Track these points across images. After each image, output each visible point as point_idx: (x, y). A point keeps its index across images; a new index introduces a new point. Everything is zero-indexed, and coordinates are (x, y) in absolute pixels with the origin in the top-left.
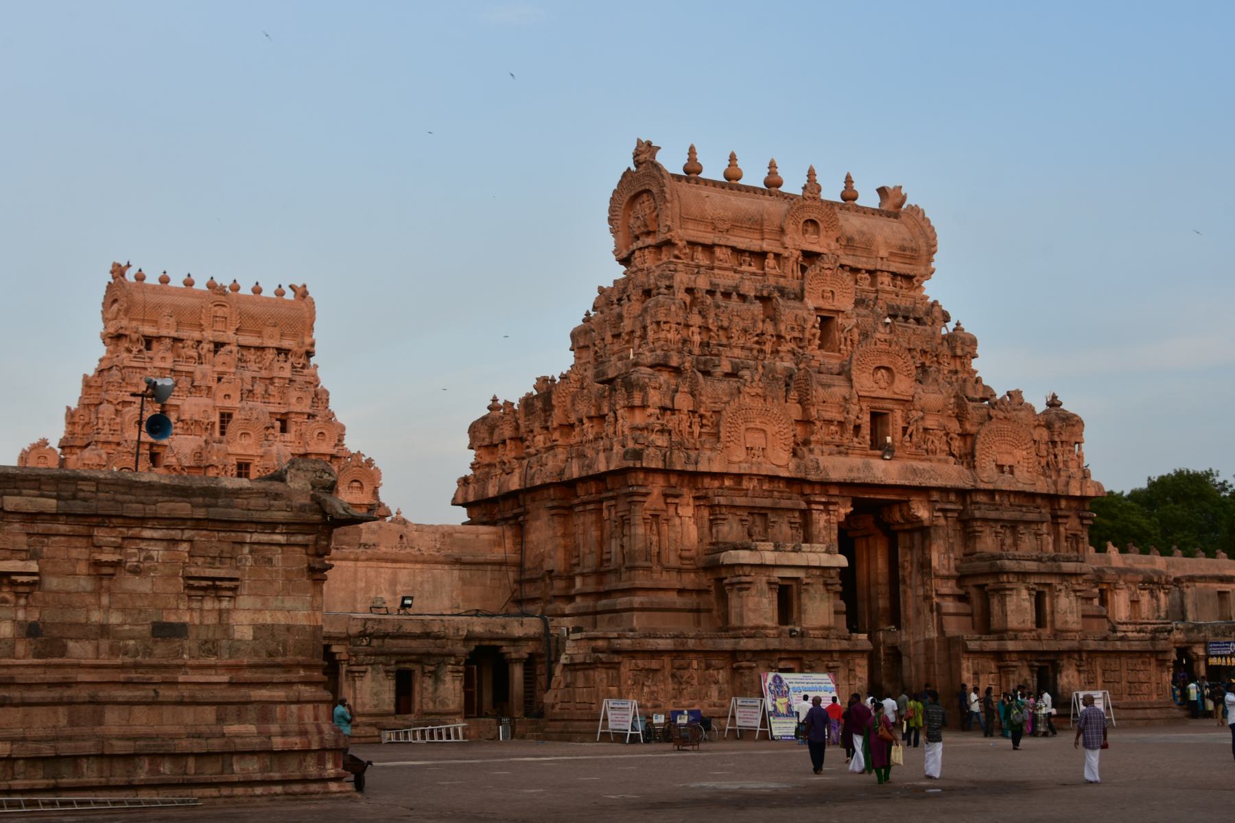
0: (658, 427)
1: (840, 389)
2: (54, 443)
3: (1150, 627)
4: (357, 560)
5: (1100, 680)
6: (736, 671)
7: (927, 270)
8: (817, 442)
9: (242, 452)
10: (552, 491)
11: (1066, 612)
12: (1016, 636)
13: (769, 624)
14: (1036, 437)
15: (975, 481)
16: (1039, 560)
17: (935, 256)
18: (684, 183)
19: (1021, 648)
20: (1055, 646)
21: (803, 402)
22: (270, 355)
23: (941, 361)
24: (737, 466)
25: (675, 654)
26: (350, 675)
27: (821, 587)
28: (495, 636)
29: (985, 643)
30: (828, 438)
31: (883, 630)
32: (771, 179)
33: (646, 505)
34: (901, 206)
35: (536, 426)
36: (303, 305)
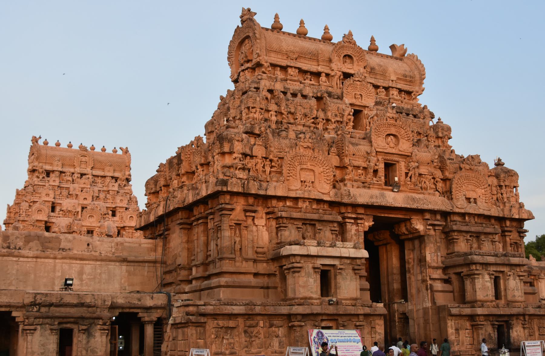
0: (240, 166)
1: (364, 147)
4: (55, 258)
5: (537, 334)
6: (291, 328)
7: (420, 89)
8: (350, 180)
9: (89, 225)
11: (514, 289)
12: (482, 305)
13: (314, 296)
14: (490, 183)
15: (453, 207)
16: (496, 255)
17: (424, 81)
18: (270, 32)
19: (486, 313)
20: (508, 311)
21: (340, 155)
23: (429, 140)
24: (294, 192)
25: (247, 317)
26: (25, 332)
27: (351, 271)
28: (133, 306)
29: (462, 310)
30: (357, 178)
31: (397, 303)
32: (325, 36)
33: (231, 216)
34: (404, 55)
35: (174, 176)
36: (126, 157)
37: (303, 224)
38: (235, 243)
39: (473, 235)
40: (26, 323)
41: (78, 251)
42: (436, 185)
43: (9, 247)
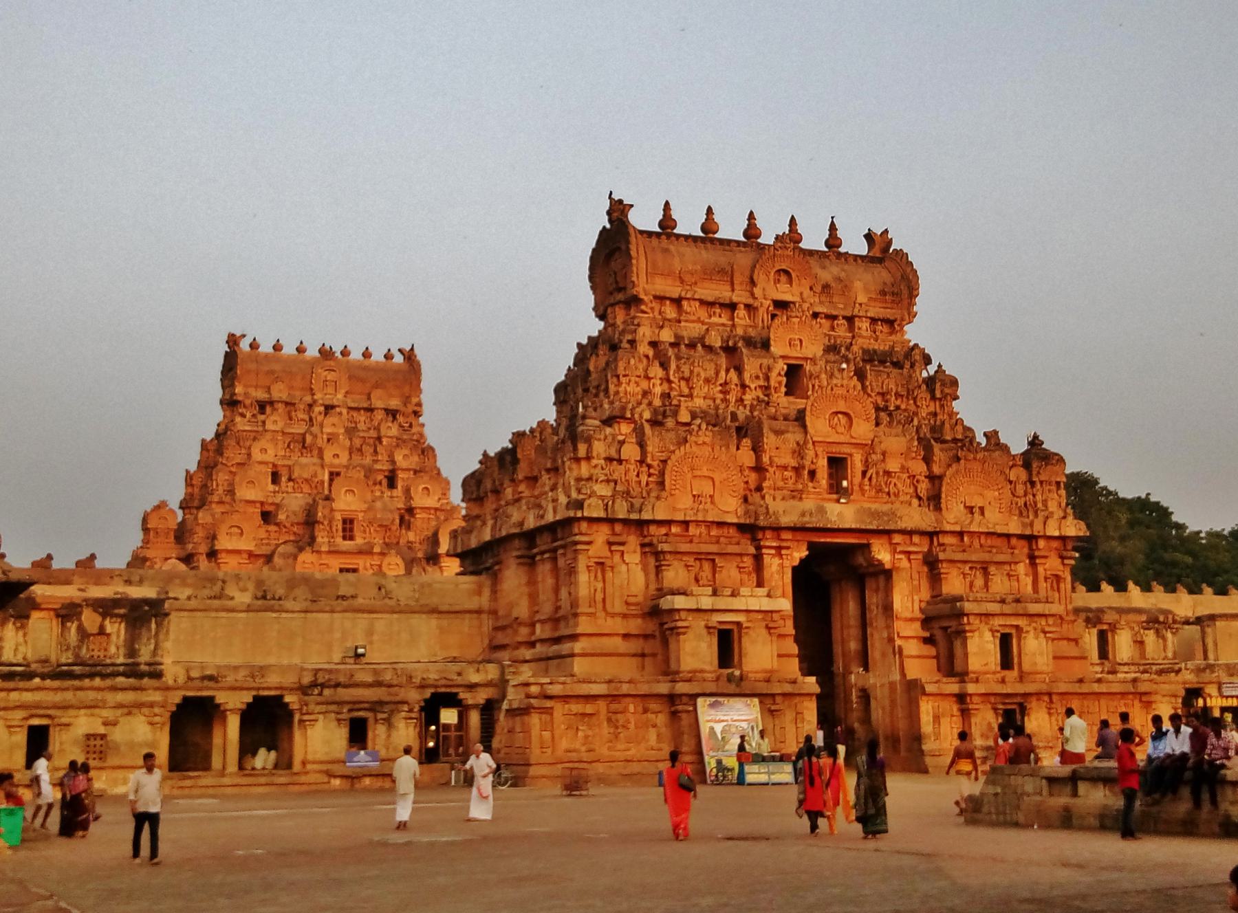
0: (603, 478)
1: (793, 436)
2: (174, 504)
3: (1154, 668)
4: (332, 611)
8: (769, 488)
10: (517, 542)
13: (707, 668)
19: (983, 691)
20: (1020, 689)
21: (757, 449)
22: (379, 415)
25: (610, 699)
37: (696, 559)
38: (595, 590)
39: (974, 565)
40: (304, 711)
41: (364, 599)
42: (916, 488)
43: (264, 597)
